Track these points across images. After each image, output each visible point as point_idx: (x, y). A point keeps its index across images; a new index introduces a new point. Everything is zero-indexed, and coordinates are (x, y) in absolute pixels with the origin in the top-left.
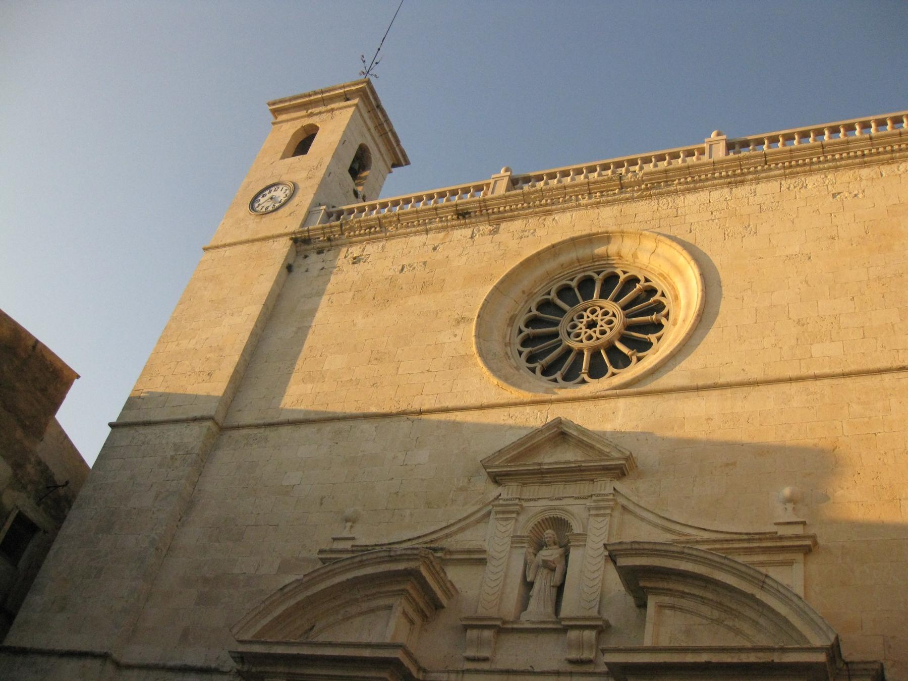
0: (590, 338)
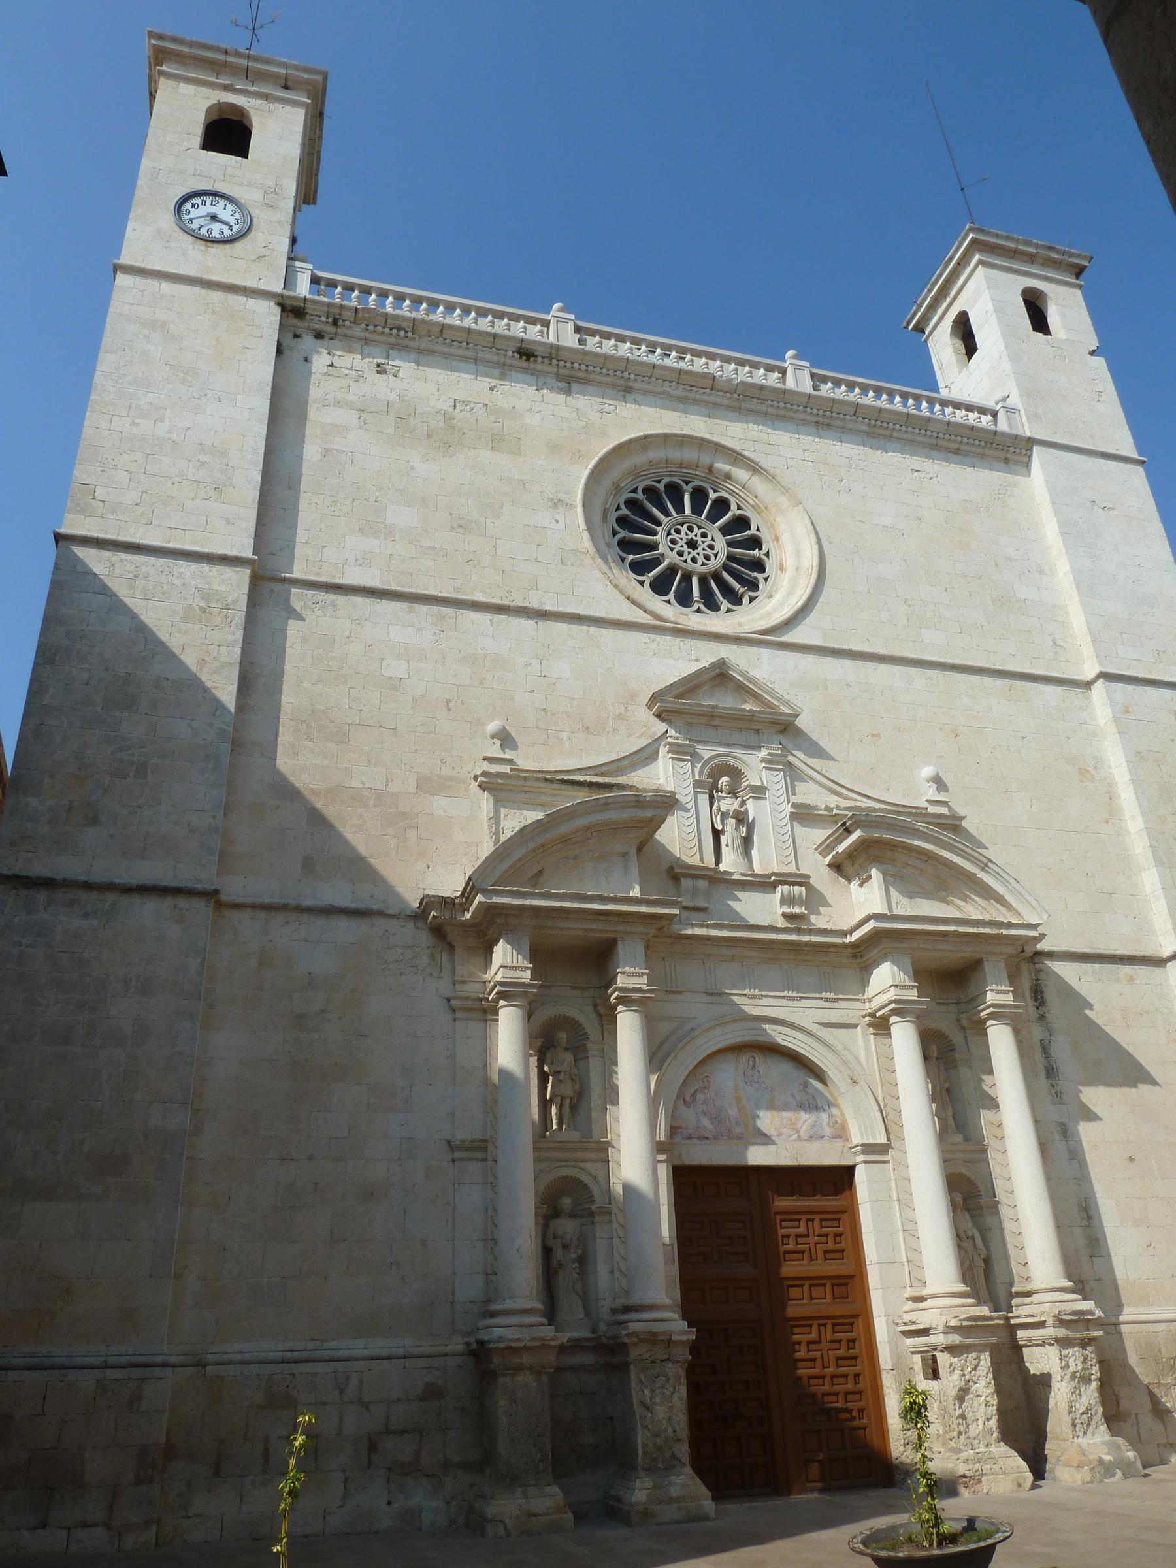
0: (680, 554)
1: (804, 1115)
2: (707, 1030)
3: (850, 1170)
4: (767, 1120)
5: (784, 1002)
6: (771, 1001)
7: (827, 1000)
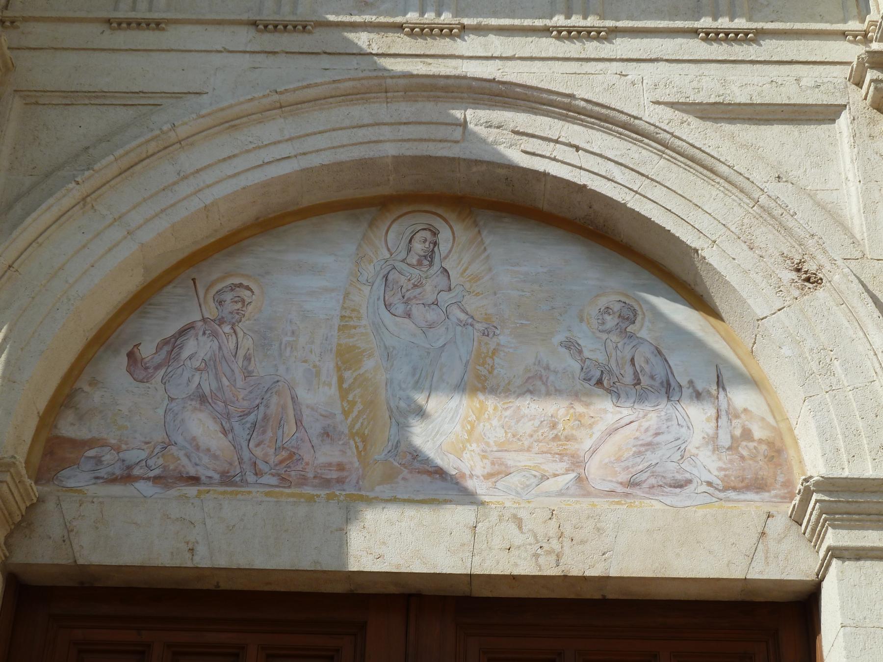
1: (607, 412)
2: (232, 123)
3: (799, 609)
4: (450, 427)
5: (549, 46)
6: (497, 44)
7: (711, 36)
